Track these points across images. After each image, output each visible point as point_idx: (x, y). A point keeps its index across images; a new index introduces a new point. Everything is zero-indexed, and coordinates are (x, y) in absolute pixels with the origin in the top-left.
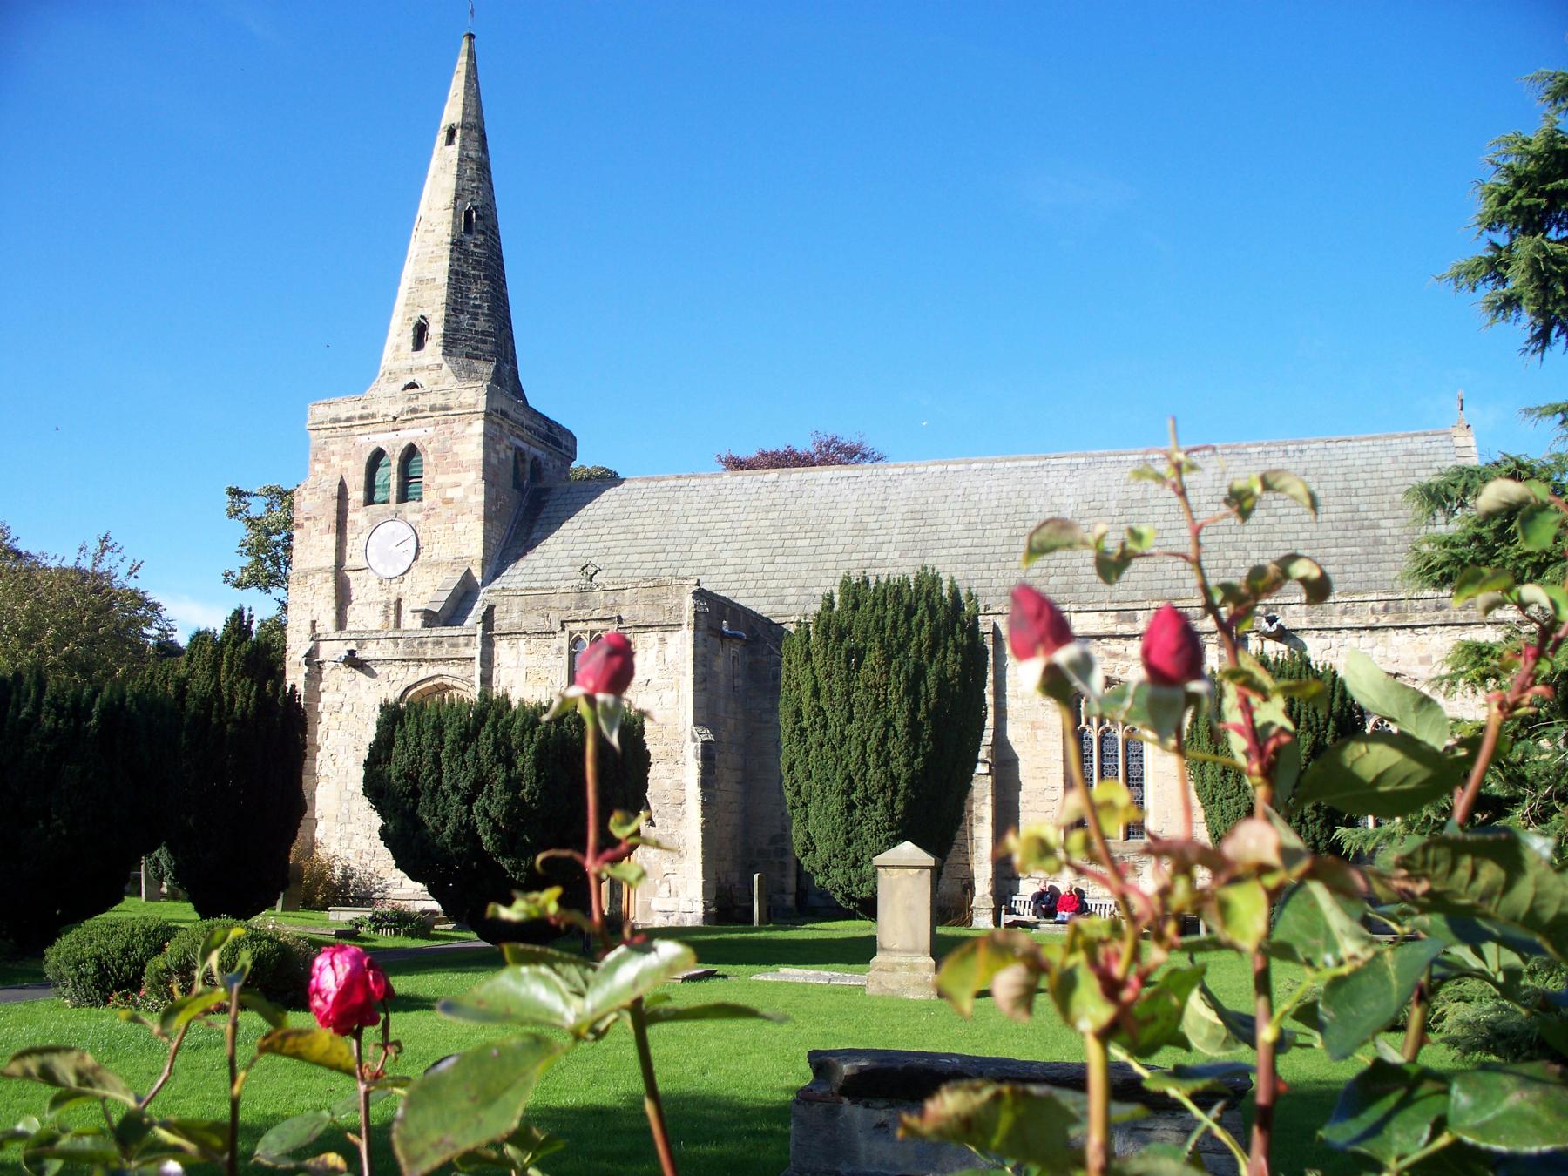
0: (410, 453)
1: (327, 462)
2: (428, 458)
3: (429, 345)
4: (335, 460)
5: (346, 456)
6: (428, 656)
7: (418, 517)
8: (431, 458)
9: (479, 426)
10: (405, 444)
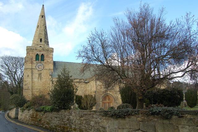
0: (42, 55)
1: (29, 54)
2: (45, 56)
5: (32, 54)
10: (42, 54)
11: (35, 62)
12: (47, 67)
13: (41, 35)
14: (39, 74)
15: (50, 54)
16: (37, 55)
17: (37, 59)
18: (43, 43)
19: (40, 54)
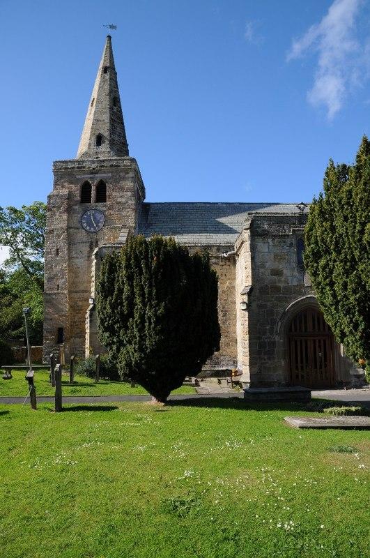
14: (91, 243)
18: (105, 147)
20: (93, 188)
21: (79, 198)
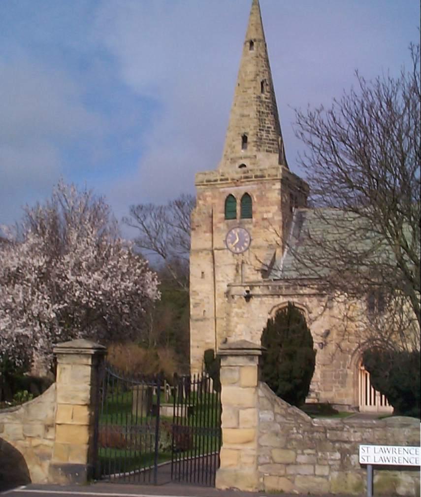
0: (247, 197)
1: (205, 200)
2: (255, 199)
3: (249, 147)
4: (209, 199)
5: (214, 197)
6: (284, 293)
7: (251, 226)
8: (255, 199)
9: (278, 186)
10: (243, 193)
11: (222, 226)
12: (259, 241)
13: (245, 120)
14: (237, 265)
15: (270, 190)
16: (230, 199)
17: (229, 213)
18: (251, 149)
19: (238, 192)
20: (238, 201)
21: (223, 215)
